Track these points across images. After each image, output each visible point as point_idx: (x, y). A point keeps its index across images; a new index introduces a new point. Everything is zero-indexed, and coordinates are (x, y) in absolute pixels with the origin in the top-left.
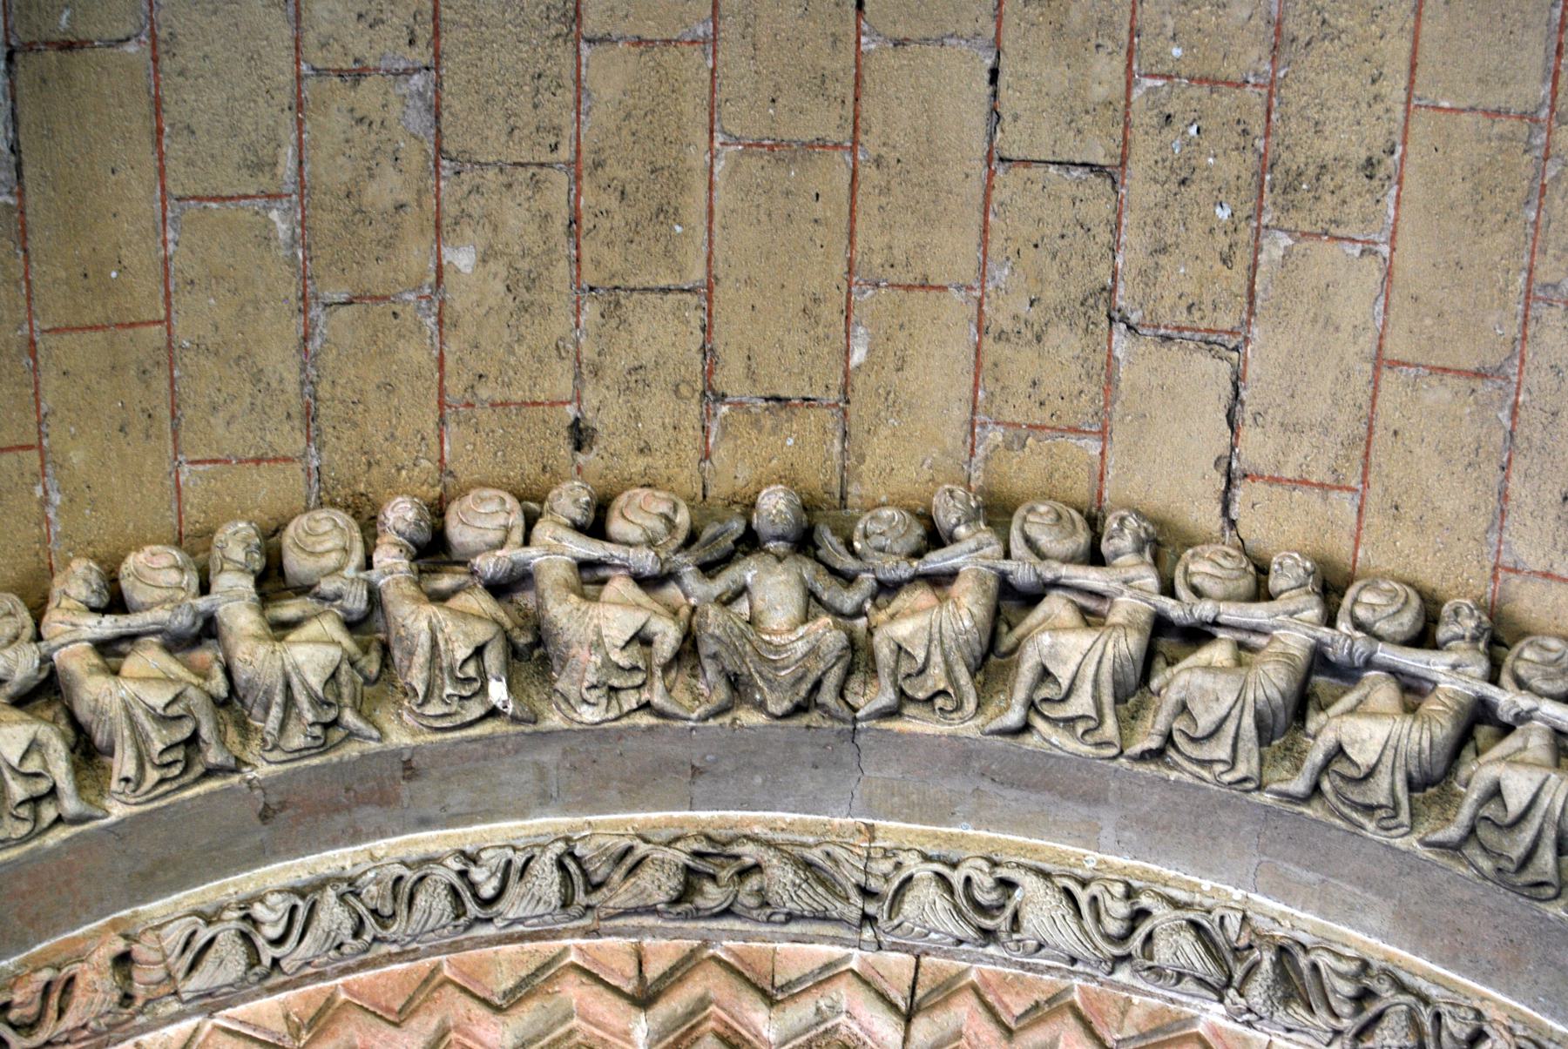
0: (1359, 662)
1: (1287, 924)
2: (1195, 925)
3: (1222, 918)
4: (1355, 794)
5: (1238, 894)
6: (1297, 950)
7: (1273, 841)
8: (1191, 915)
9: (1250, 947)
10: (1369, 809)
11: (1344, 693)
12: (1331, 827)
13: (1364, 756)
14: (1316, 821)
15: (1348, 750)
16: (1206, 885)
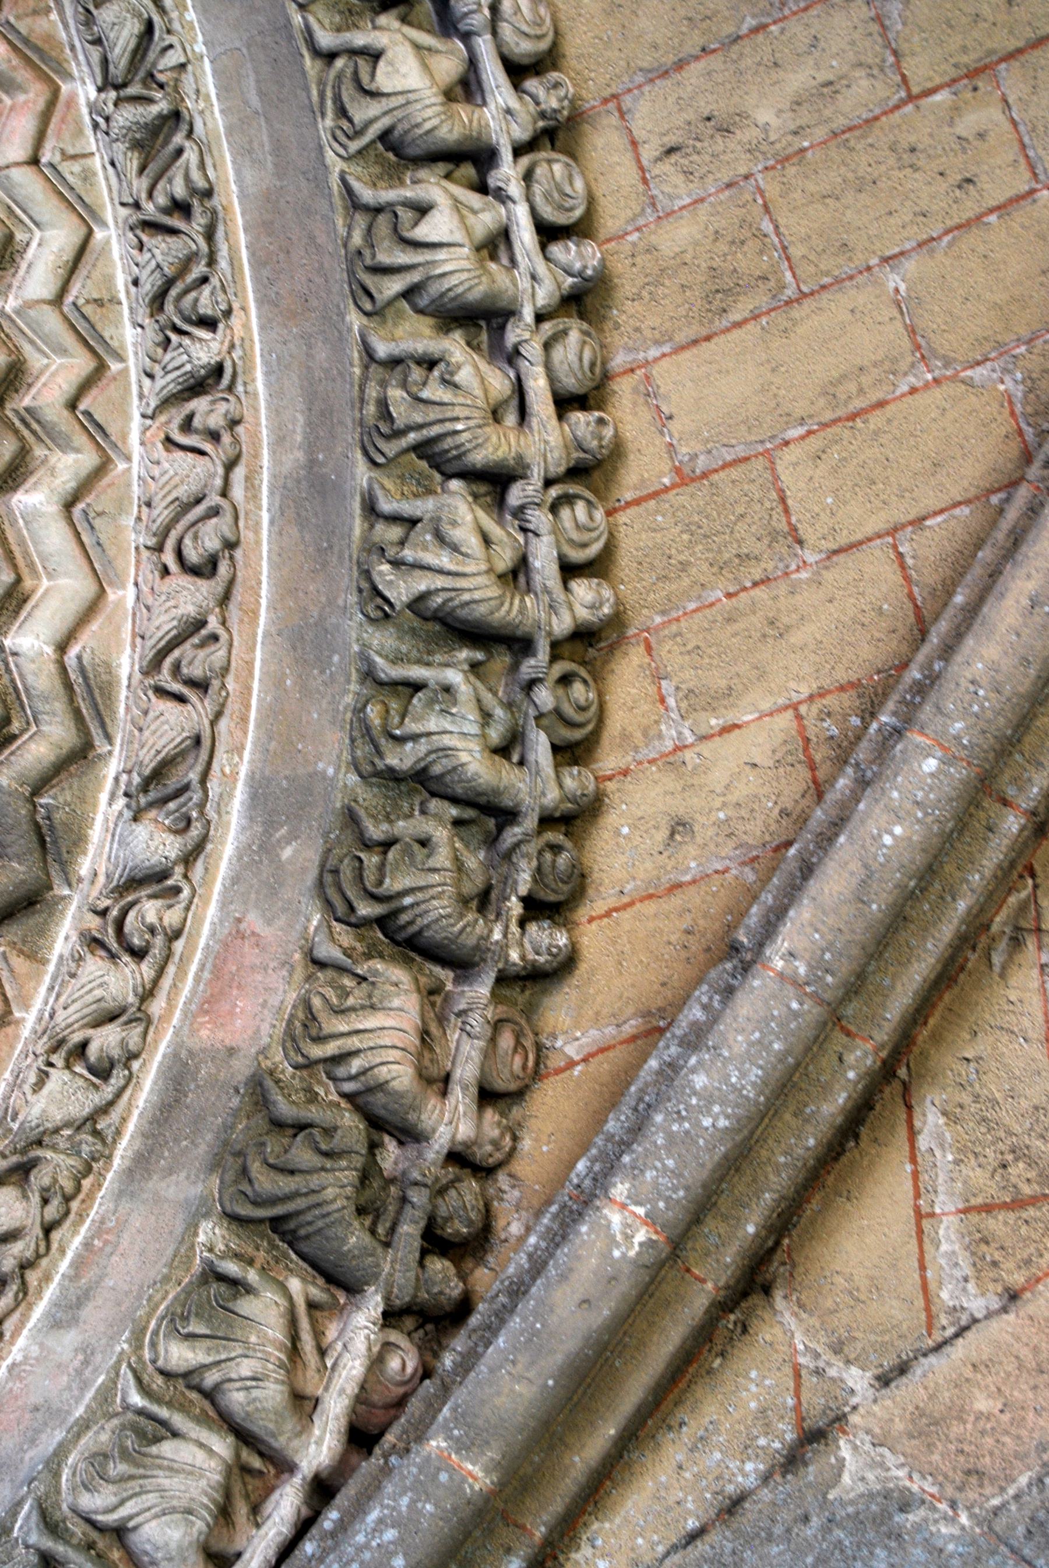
0: (463, 27)
1: (202, 105)
2: (149, 27)
3: (171, 46)
4: (348, 93)
5: (200, 48)
6: (186, 127)
7: (264, 47)
8: (156, 18)
9: (161, 86)
10: (342, 112)
11: (428, 31)
12: (307, 89)
13: (385, 79)
14: (304, 73)
15: (382, 64)
16: (191, 15)
